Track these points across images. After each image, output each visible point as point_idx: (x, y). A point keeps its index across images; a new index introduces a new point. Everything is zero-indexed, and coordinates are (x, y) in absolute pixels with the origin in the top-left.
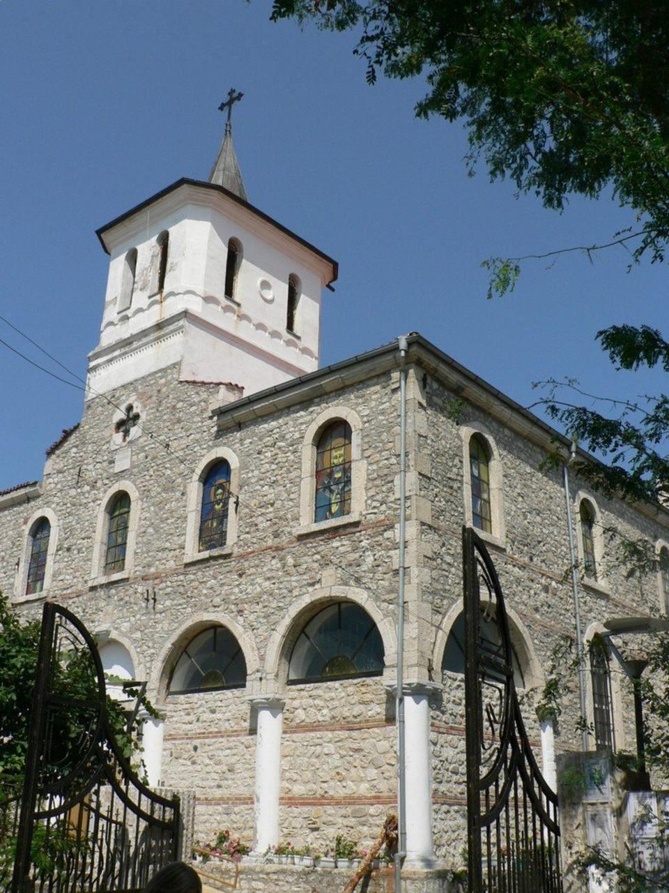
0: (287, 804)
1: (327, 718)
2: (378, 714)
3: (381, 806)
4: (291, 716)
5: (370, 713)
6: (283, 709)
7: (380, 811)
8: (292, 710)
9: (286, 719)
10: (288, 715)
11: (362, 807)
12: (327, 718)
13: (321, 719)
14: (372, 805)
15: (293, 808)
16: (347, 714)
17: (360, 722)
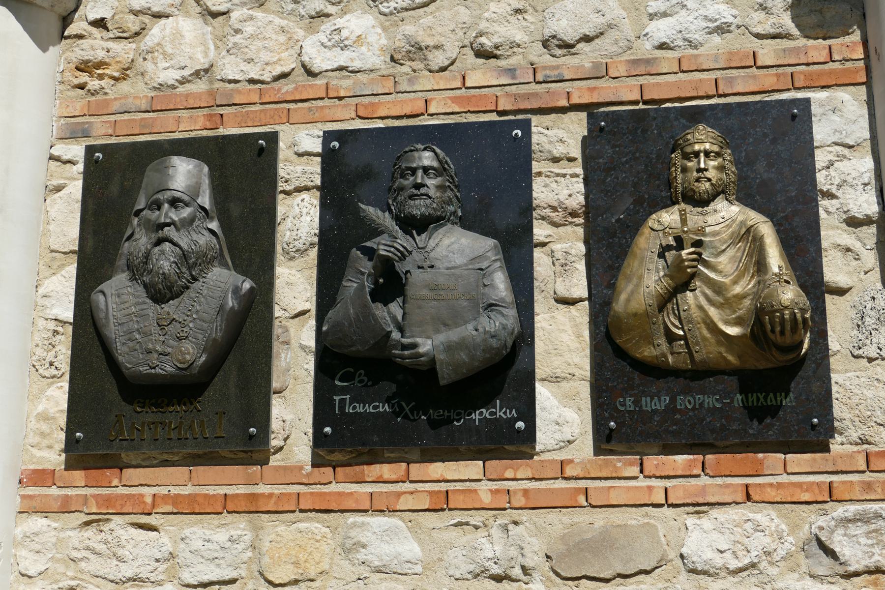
0: (65, 508)
1: (370, 55)
2: (722, 29)
3: (765, 516)
4: (124, 51)
5: (661, 30)
6: (66, 20)
7: (759, 542)
8: (132, 24)
9: (84, 67)
10: (96, 46)
11: (633, 518)
12: (370, 55)
13: (322, 59)
14: (700, 507)
15: (119, 528)
16: (515, 31)
17: (601, 72)
